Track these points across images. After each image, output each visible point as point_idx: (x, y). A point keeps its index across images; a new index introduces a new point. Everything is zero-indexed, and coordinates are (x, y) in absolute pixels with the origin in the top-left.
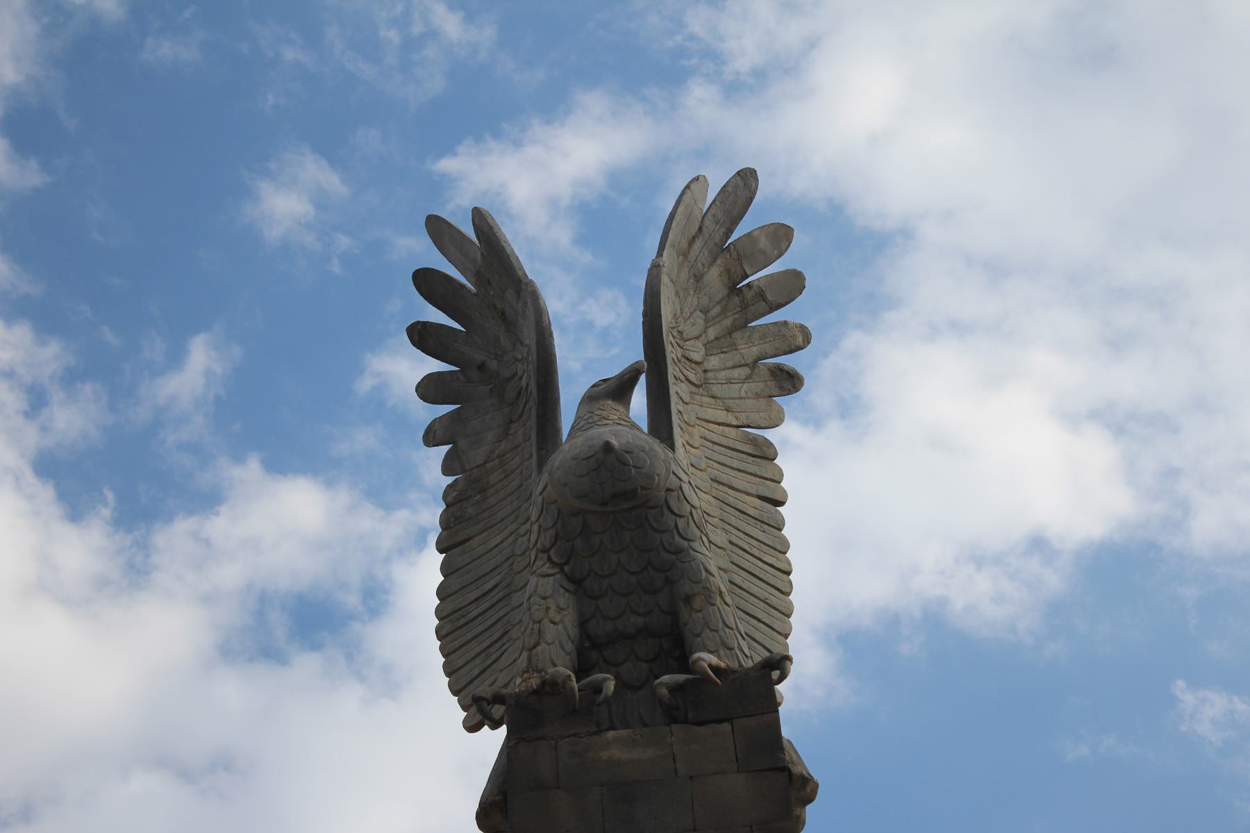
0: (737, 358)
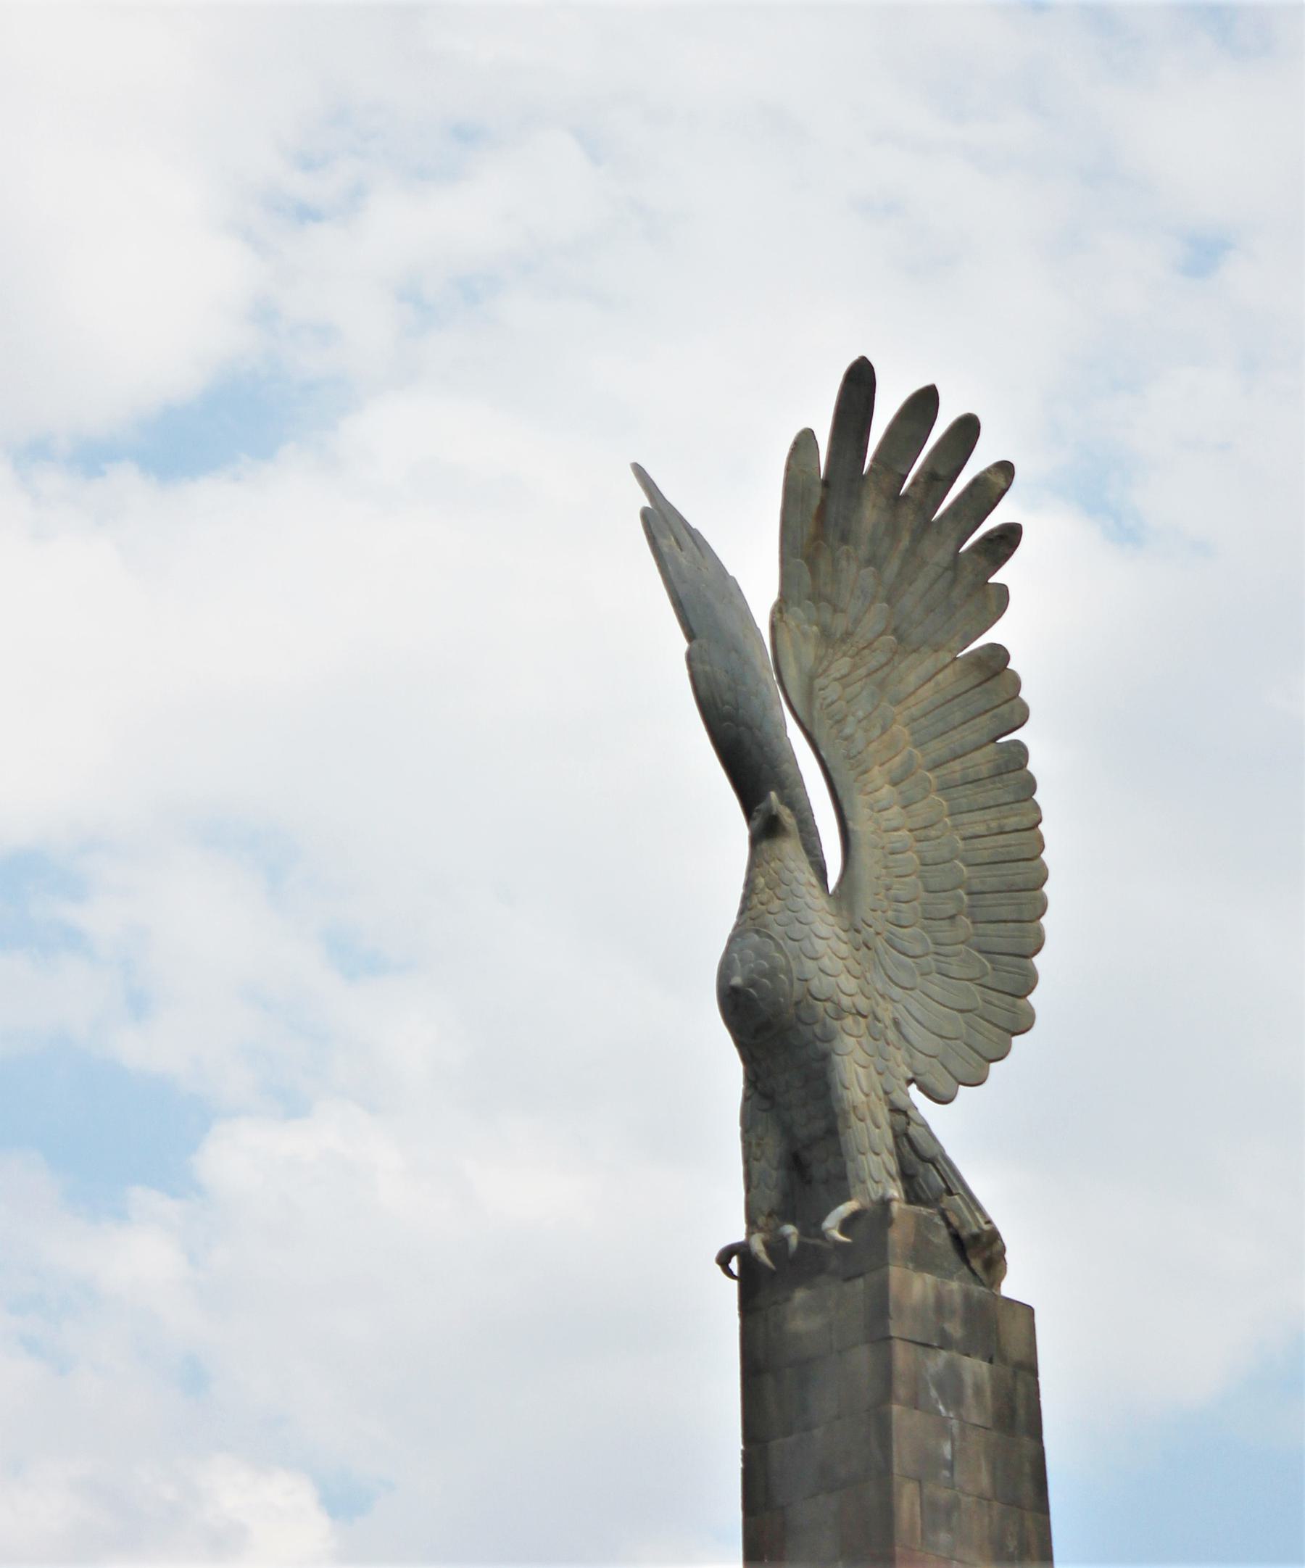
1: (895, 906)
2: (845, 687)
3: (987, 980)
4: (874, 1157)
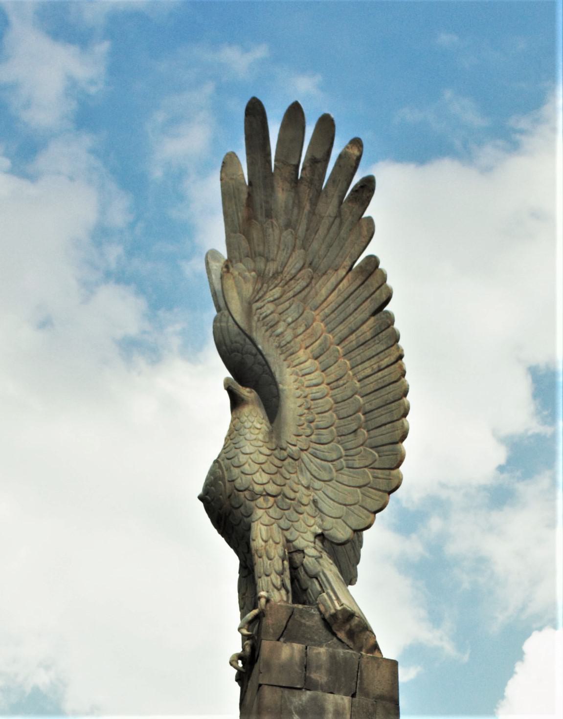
0: (326, 222)
1: (316, 432)
2: (277, 305)
3: (376, 465)
4: (266, 578)
